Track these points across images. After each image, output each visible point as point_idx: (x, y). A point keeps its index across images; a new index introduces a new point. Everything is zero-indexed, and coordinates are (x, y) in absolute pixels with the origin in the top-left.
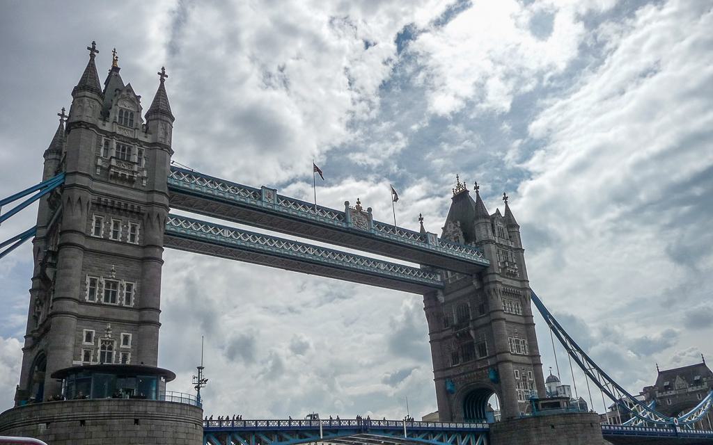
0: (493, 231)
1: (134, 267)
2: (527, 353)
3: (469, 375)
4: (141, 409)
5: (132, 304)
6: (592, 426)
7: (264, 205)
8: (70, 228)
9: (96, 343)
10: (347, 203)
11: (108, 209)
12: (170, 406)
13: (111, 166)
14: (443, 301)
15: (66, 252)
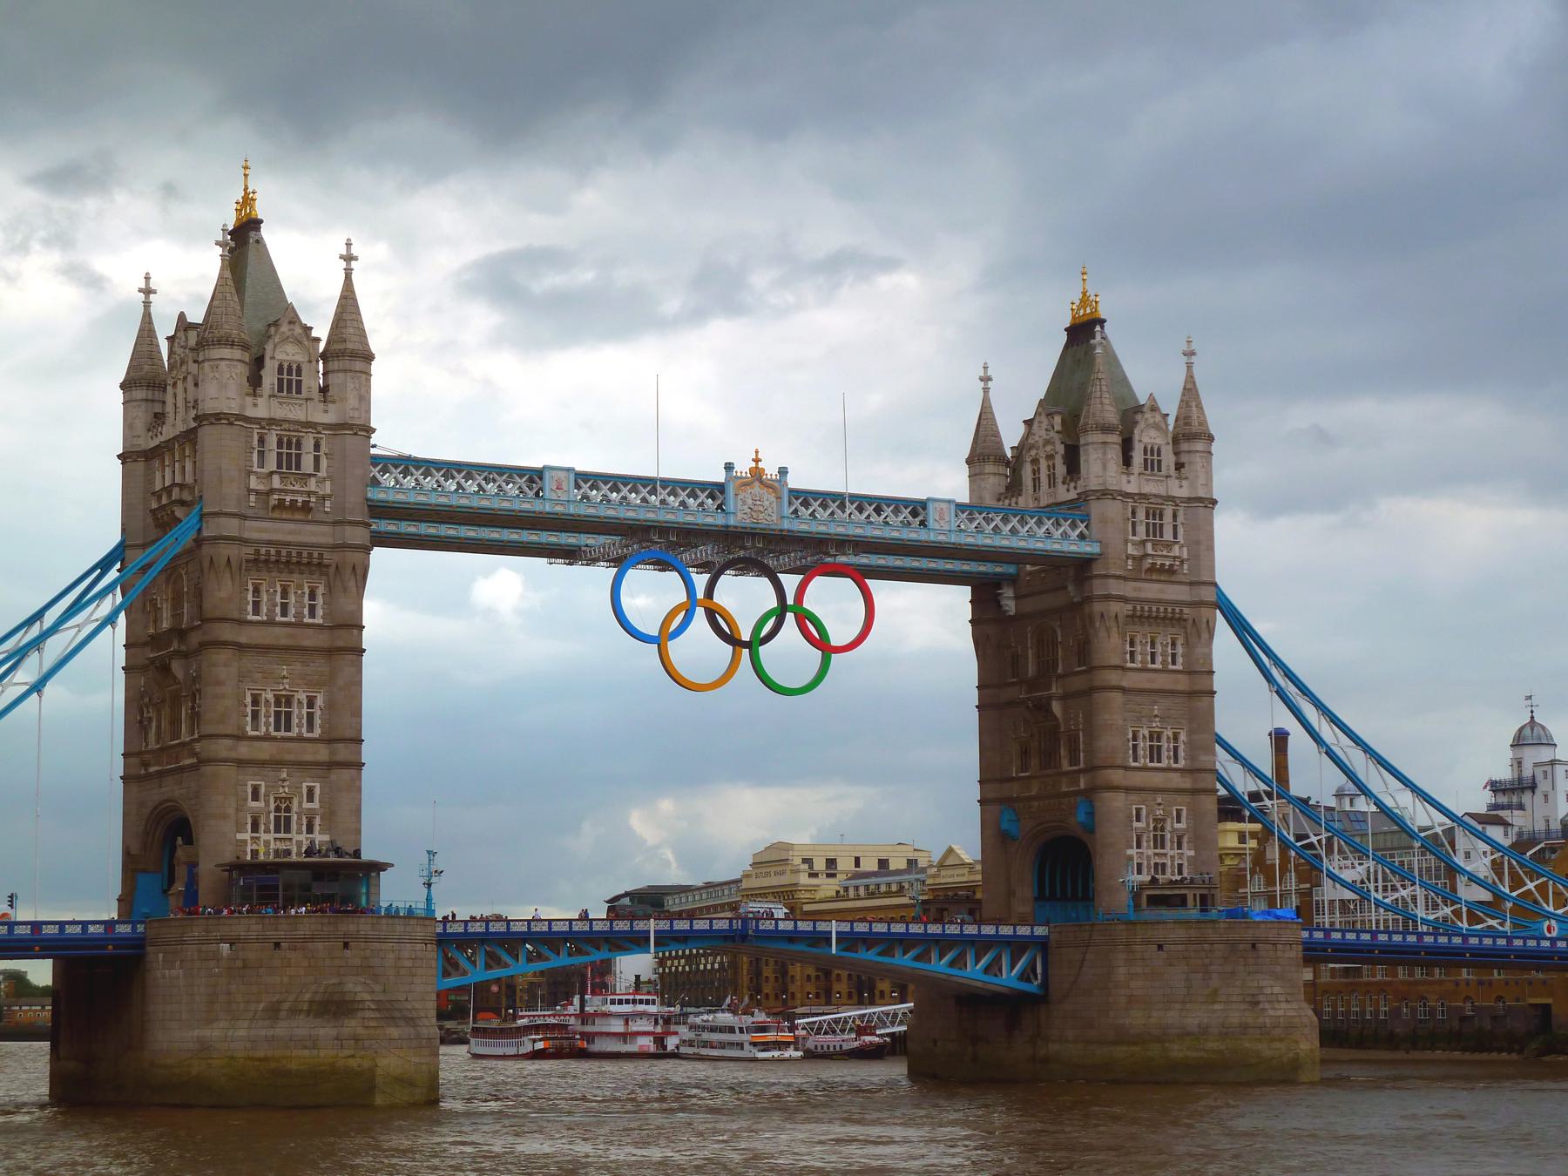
0: (1127, 461)
1: (319, 666)
2: (1183, 762)
3: (1047, 802)
4: (352, 928)
5: (317, 732)
6: (1254, 946)
7: (548, 509)
8: (218, 614)
9: (267, 803)
10: (729, 467)
11: (271, 566)
12: (390, 921)
13: (272, 491)
14: (1012, 612)
15: (214, 656)
